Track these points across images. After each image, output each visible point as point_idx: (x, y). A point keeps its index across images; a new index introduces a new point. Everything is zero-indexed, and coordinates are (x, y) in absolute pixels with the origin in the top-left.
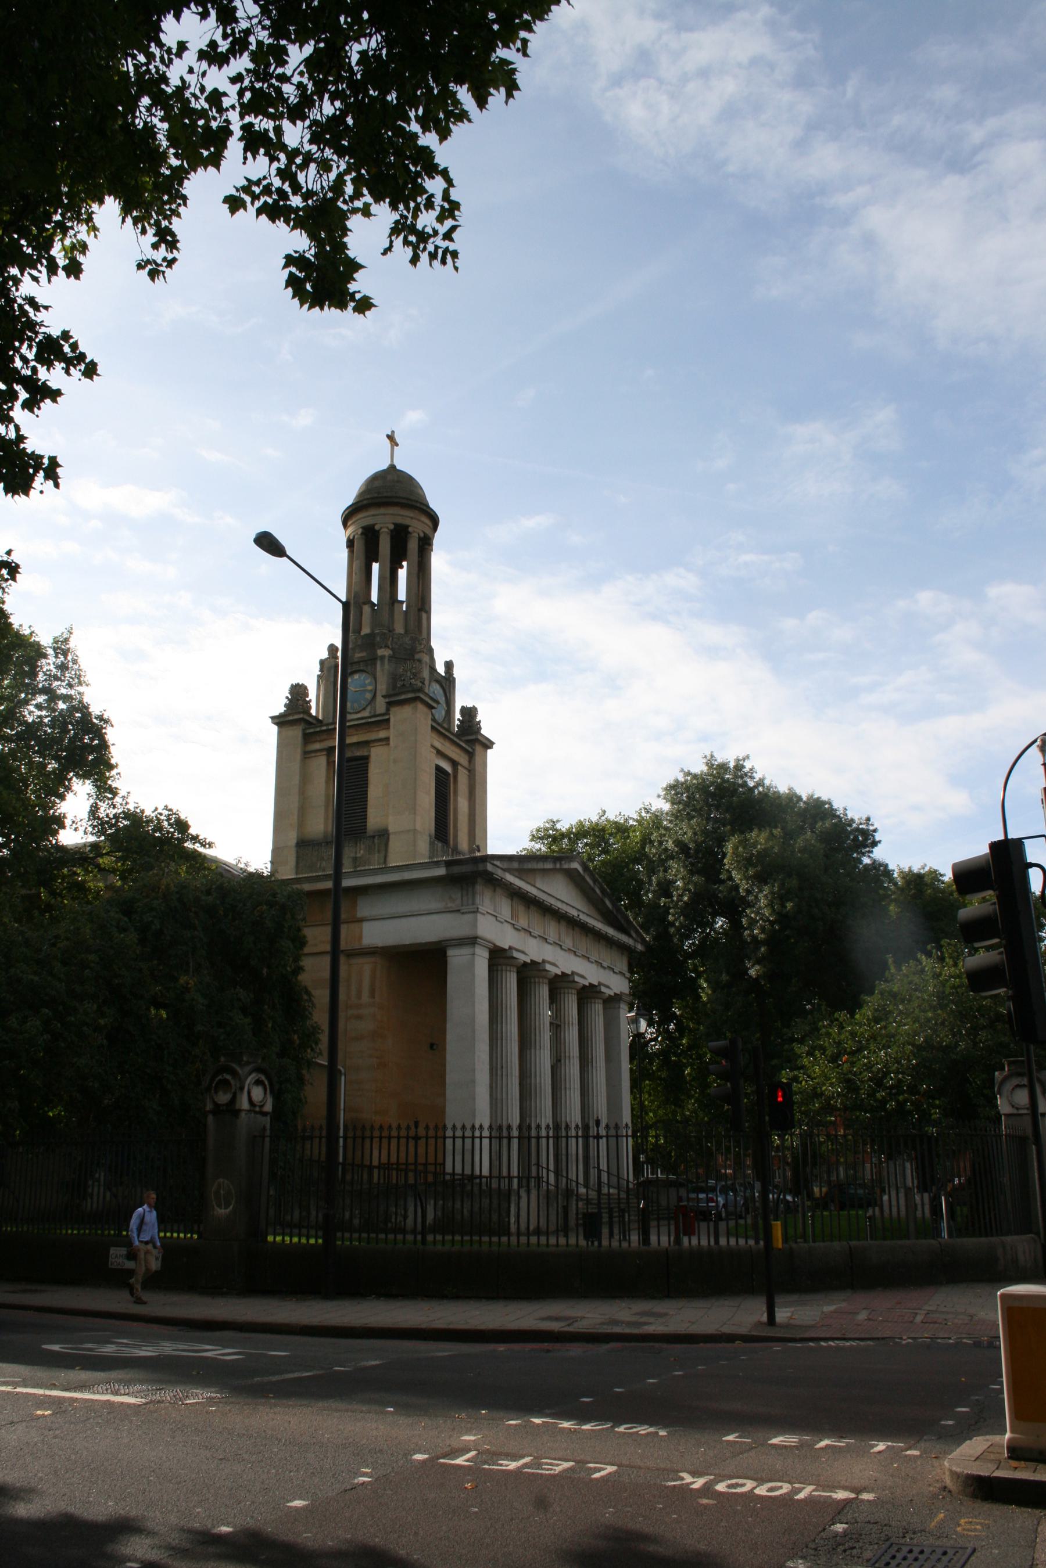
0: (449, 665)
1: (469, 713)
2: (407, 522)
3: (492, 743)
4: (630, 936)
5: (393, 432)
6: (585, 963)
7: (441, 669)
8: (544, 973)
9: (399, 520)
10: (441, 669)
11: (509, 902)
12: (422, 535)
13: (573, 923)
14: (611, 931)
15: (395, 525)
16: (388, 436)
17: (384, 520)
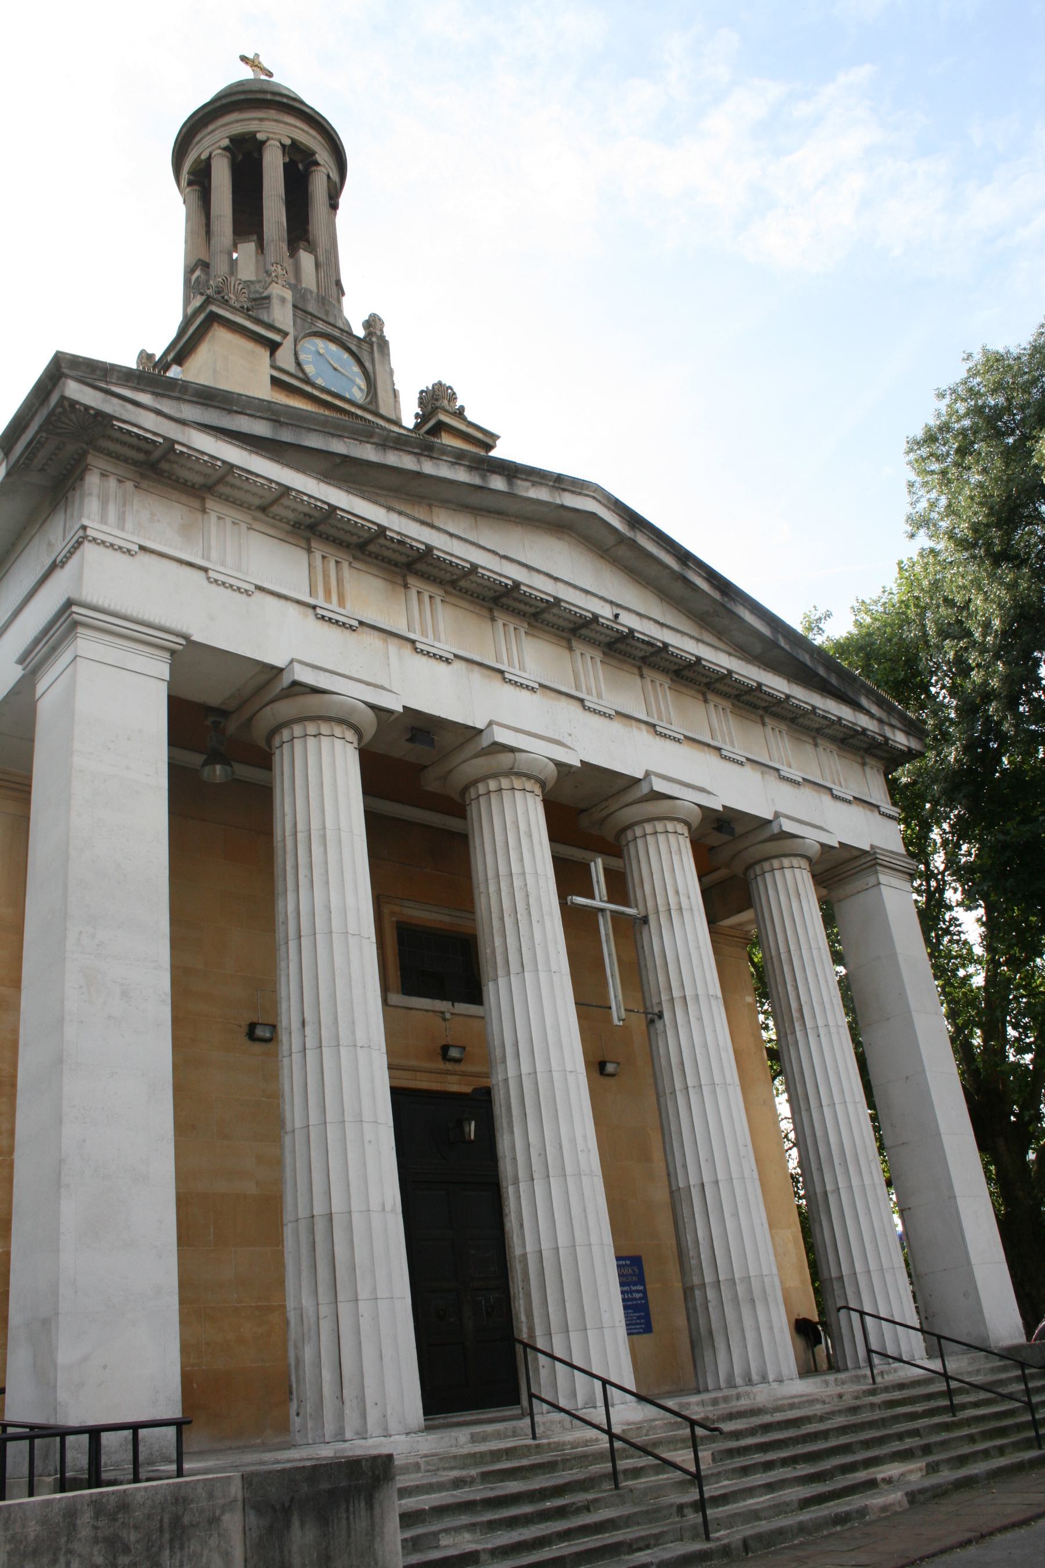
0: (373, 324)
1: (436, 400)
2: (253, 126)
3: (494, 437)
4: (857, 706)
5: (257, 55)
6: (711, 759)
7: (359, 332)
8: (505, 760)
9: (238, 129)
10: (359, 332)
11: (303, 555)
12: (288, 142)
13: (623, 650)
14: (777, 684)
15: (233, 139)
16: (243, 59)
17: (213, 142)
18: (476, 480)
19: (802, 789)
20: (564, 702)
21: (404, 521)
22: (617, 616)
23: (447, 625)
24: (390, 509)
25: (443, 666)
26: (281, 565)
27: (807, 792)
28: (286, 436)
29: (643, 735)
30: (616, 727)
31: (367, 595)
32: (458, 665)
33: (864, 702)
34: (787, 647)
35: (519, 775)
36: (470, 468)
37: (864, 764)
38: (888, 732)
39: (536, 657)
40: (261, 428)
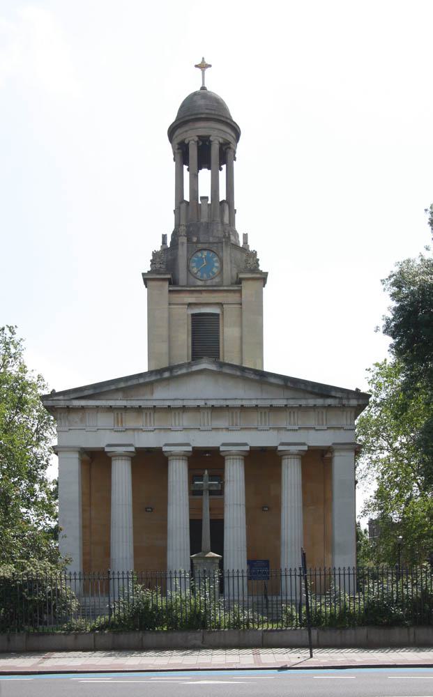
18: (159, 377)
19: (299, 431)
20: (192, 432)
21: (132, 401)
22: (206, 404)
23: (158, 421)
24: (127, 400)
25: (152, 433)
26: (106, 420)
27: (302, 432)
28: (98, 391)
29: (224, 432)
30: (214, 433)
31: (131, 421)
32: (156, 431)
33: (333, 394)
34: (292, 386)
35: (174, 456)
36: (156, 375)
37: (343, 411)
38: (345, 402)
39: (186, 420)
40: (90, 392)
